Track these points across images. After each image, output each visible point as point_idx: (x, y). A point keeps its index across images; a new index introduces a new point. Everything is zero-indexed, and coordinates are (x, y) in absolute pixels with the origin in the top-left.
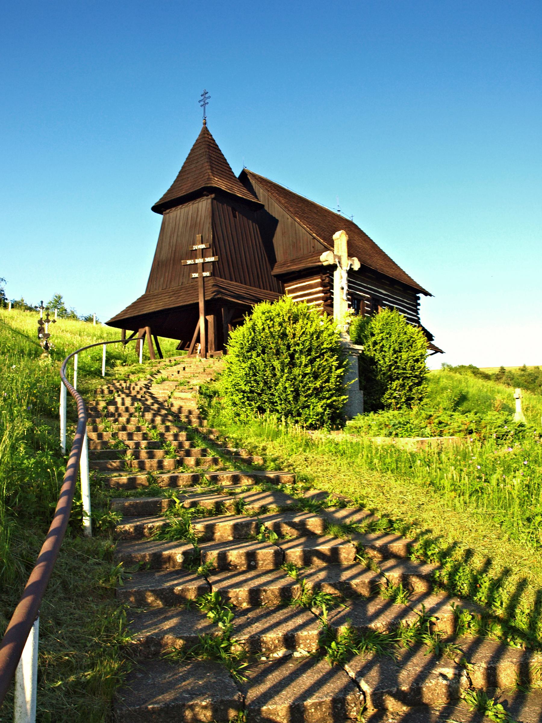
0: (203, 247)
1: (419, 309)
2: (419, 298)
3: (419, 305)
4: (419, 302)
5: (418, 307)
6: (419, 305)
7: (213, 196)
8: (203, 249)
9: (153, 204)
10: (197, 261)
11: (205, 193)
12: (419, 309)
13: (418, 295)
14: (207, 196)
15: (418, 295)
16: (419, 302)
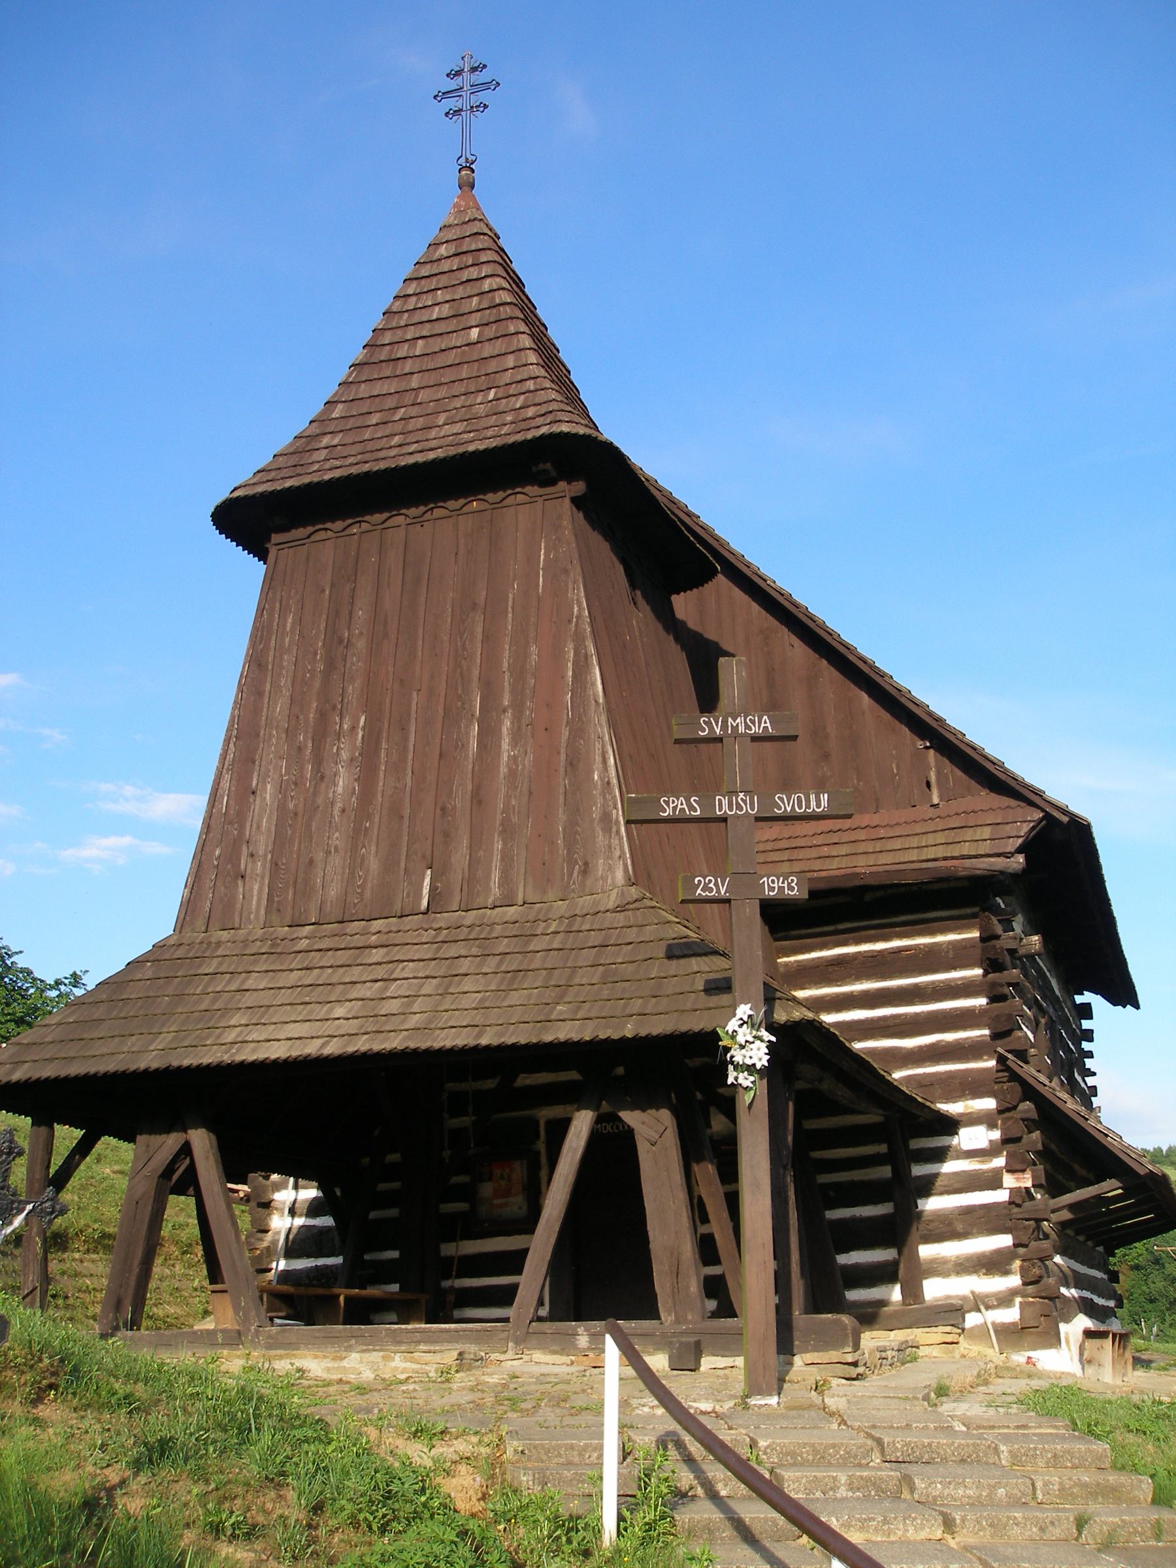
0: (754, 730)
1: (1090, 1055)
2: (1086, 1011)
3: (1088, 1035)
4: (1086, 1024)
5: (1086, 1046)
6: (1088, 1035)
7: (579, 487)
8: (755, 739)
9: (222, 494)
10: (723, 806)
11: (548, 466)
12: (1090, 1055)
13: (1079, 999)
14: (547, 481)
15: (1079, 999)
16: (1086, 1024)
